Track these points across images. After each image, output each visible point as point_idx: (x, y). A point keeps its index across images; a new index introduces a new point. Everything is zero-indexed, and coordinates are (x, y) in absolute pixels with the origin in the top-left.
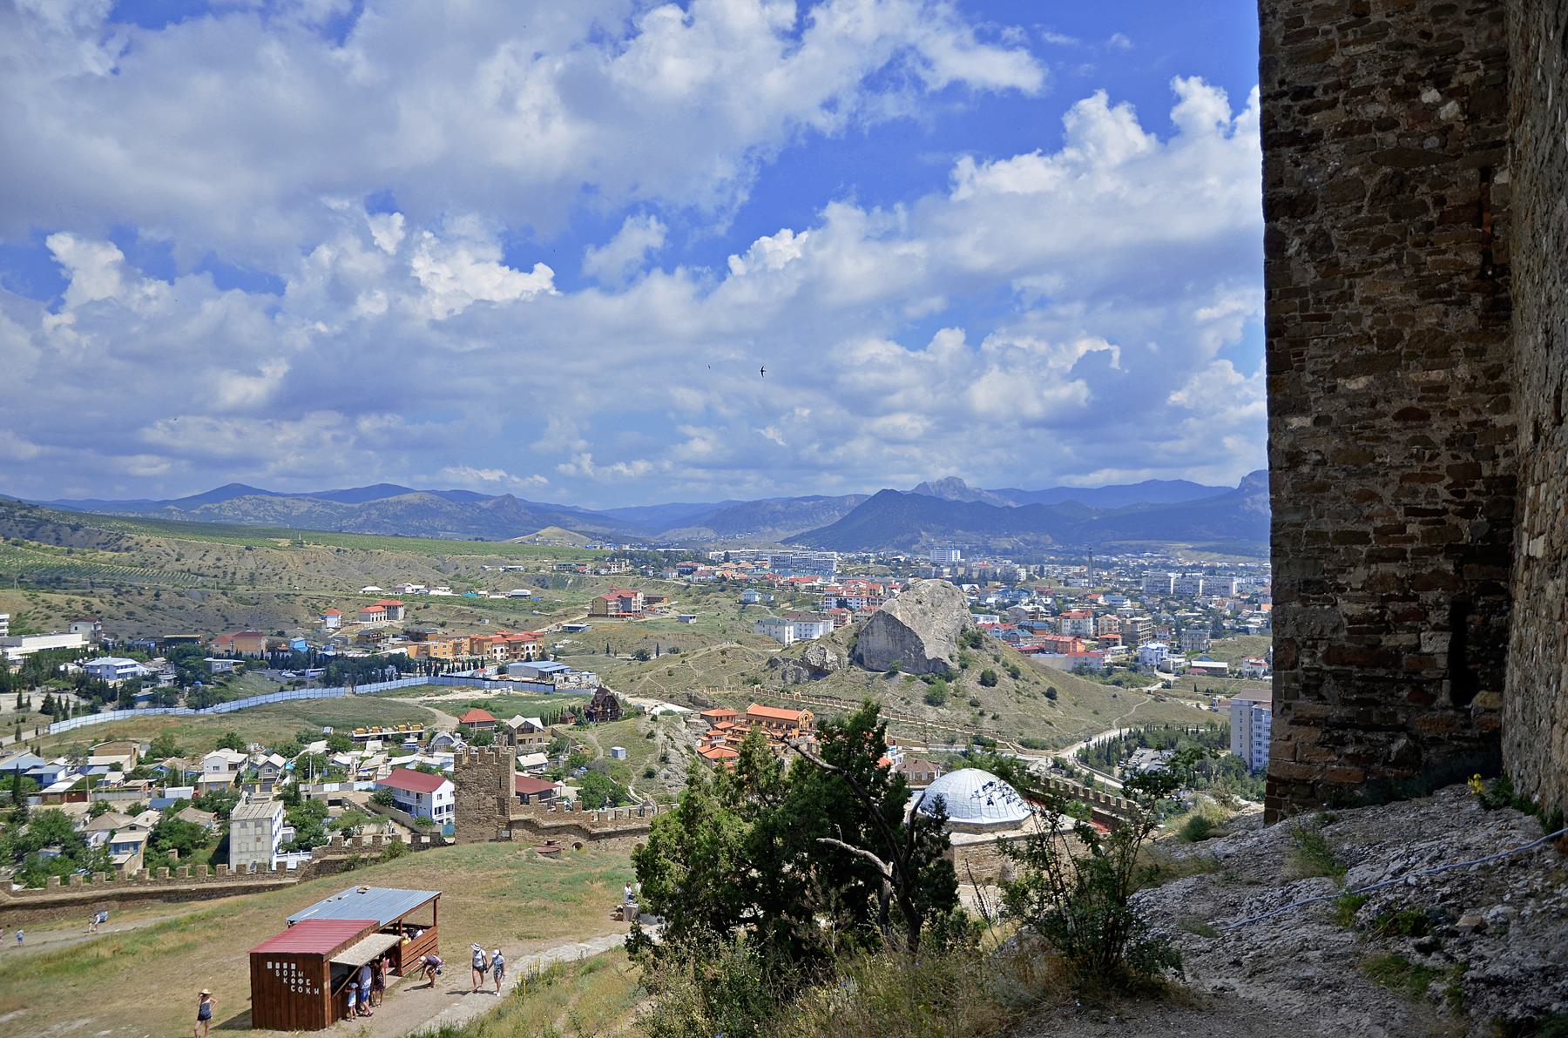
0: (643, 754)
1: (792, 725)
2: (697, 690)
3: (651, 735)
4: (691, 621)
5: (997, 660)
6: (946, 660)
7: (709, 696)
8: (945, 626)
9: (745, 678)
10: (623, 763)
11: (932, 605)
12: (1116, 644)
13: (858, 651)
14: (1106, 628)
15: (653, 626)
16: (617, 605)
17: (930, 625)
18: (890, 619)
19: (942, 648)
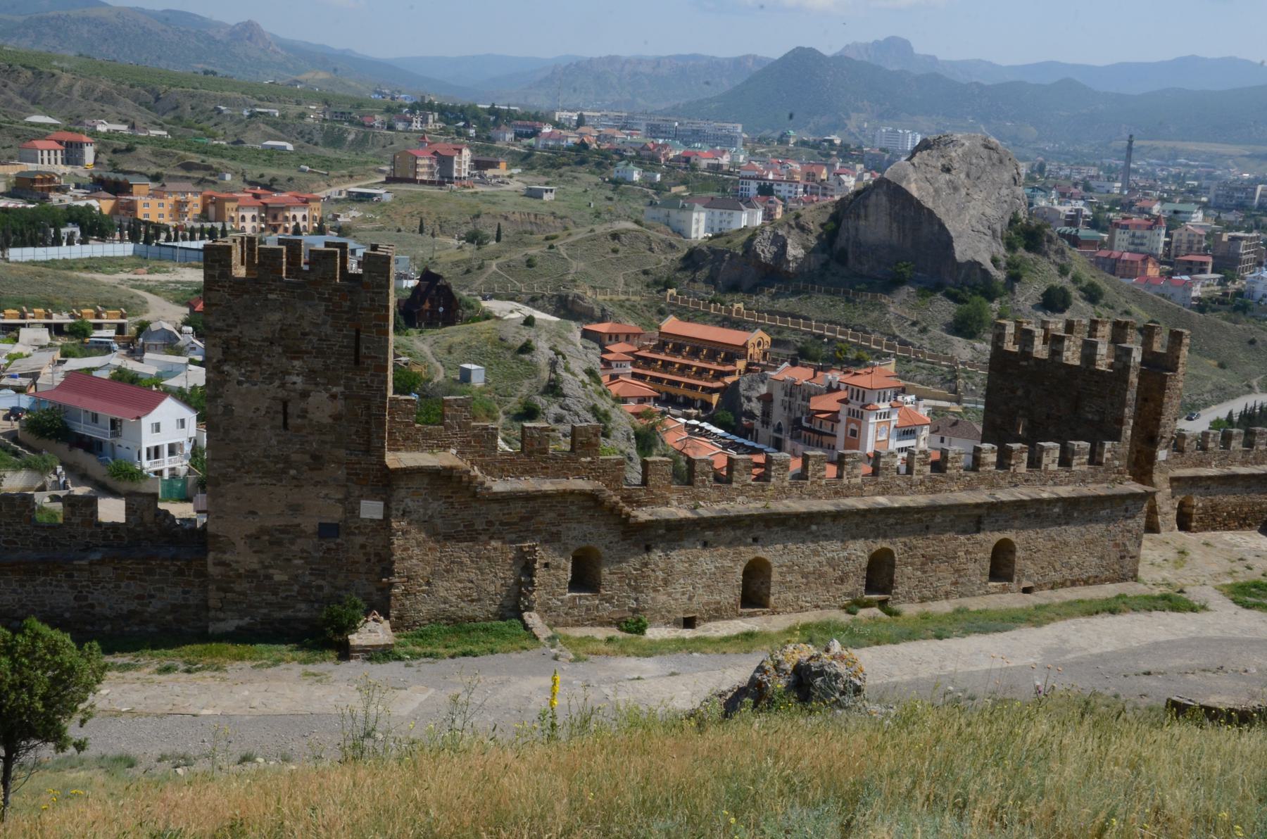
0: (514, 377)
1: (733, 354)
2: (576, 291)
3: (527, 348)
4: (547, 197)
5: (1063, 271)
6: (989, 265)
7: (595, 301)
8: (989, 211)
9: (650, 279)
10: (481, 391)
11: (968, 175)
12: (1203, 271)
13: (840, 243)
14: (1184, 247)
15: (491, 200)
16: (431, 166)
17: (962, 209)
18: (897, 193)
19: (982, 246)
